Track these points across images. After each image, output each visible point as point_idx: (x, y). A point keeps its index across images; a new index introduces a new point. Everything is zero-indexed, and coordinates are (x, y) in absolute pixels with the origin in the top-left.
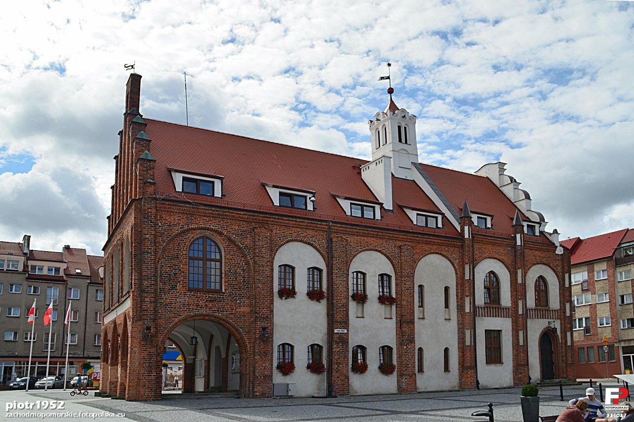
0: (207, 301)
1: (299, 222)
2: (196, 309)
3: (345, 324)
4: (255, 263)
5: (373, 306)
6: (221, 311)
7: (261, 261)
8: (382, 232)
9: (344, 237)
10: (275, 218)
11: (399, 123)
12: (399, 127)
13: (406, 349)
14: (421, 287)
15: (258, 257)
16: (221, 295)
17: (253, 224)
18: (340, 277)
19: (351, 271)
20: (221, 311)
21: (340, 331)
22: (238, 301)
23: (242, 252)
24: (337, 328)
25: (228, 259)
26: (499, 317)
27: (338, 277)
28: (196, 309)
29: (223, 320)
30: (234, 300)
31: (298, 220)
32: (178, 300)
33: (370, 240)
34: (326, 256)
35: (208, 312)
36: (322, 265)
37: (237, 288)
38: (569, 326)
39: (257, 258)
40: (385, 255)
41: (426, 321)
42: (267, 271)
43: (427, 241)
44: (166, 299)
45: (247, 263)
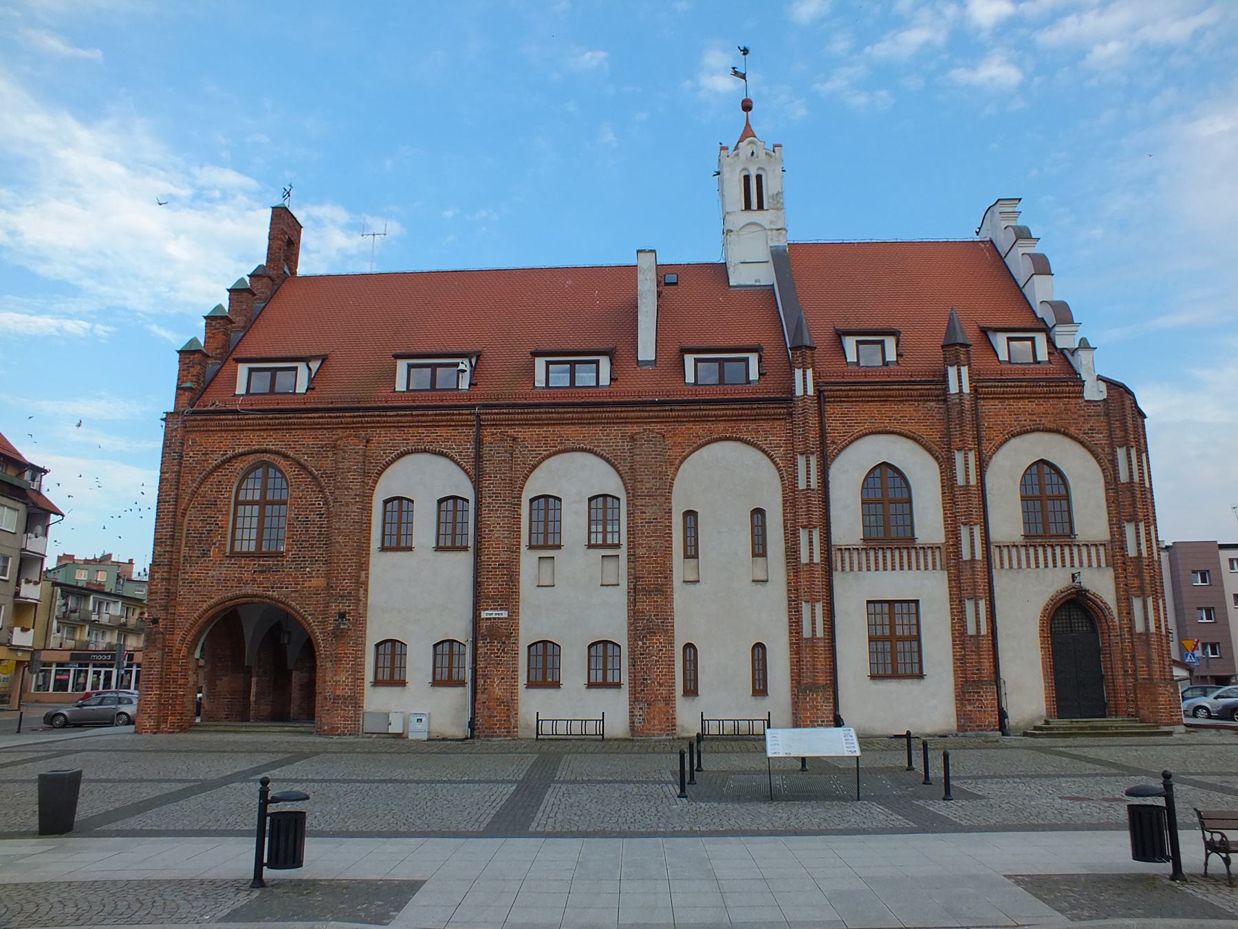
0: (255, 571)
1: (418, 415)
2: (236, 587)
3: (509, 597)
6: (277, 588)
7: (345, 495)
9: (510, 432)
10: (375, 416)
11: (744, 169)
12: (747, 178)
13: (643, 647)
14: (690, 515)
15: (339, 489)
16: (278, 561)
19: (527, 495)
20: (277, 588)
21: (494, 614)
22: (308, 569)
23: (319, 484)
24: (487, 609)
25: (295, 498)
26: (885, 569)
27: (493, 510)
28: (236, 587)
29: (281, 602)
31: (414, 413)
32: (210, 573)
33: (568, 430)
34: (472, 472)
35: (260, 591)
36: (465, 489)
37: (307, 547)
38: (1136, 582)
39: (337, 492)
40: (601, 456)
42: (355, 512)
43: (696, 417)
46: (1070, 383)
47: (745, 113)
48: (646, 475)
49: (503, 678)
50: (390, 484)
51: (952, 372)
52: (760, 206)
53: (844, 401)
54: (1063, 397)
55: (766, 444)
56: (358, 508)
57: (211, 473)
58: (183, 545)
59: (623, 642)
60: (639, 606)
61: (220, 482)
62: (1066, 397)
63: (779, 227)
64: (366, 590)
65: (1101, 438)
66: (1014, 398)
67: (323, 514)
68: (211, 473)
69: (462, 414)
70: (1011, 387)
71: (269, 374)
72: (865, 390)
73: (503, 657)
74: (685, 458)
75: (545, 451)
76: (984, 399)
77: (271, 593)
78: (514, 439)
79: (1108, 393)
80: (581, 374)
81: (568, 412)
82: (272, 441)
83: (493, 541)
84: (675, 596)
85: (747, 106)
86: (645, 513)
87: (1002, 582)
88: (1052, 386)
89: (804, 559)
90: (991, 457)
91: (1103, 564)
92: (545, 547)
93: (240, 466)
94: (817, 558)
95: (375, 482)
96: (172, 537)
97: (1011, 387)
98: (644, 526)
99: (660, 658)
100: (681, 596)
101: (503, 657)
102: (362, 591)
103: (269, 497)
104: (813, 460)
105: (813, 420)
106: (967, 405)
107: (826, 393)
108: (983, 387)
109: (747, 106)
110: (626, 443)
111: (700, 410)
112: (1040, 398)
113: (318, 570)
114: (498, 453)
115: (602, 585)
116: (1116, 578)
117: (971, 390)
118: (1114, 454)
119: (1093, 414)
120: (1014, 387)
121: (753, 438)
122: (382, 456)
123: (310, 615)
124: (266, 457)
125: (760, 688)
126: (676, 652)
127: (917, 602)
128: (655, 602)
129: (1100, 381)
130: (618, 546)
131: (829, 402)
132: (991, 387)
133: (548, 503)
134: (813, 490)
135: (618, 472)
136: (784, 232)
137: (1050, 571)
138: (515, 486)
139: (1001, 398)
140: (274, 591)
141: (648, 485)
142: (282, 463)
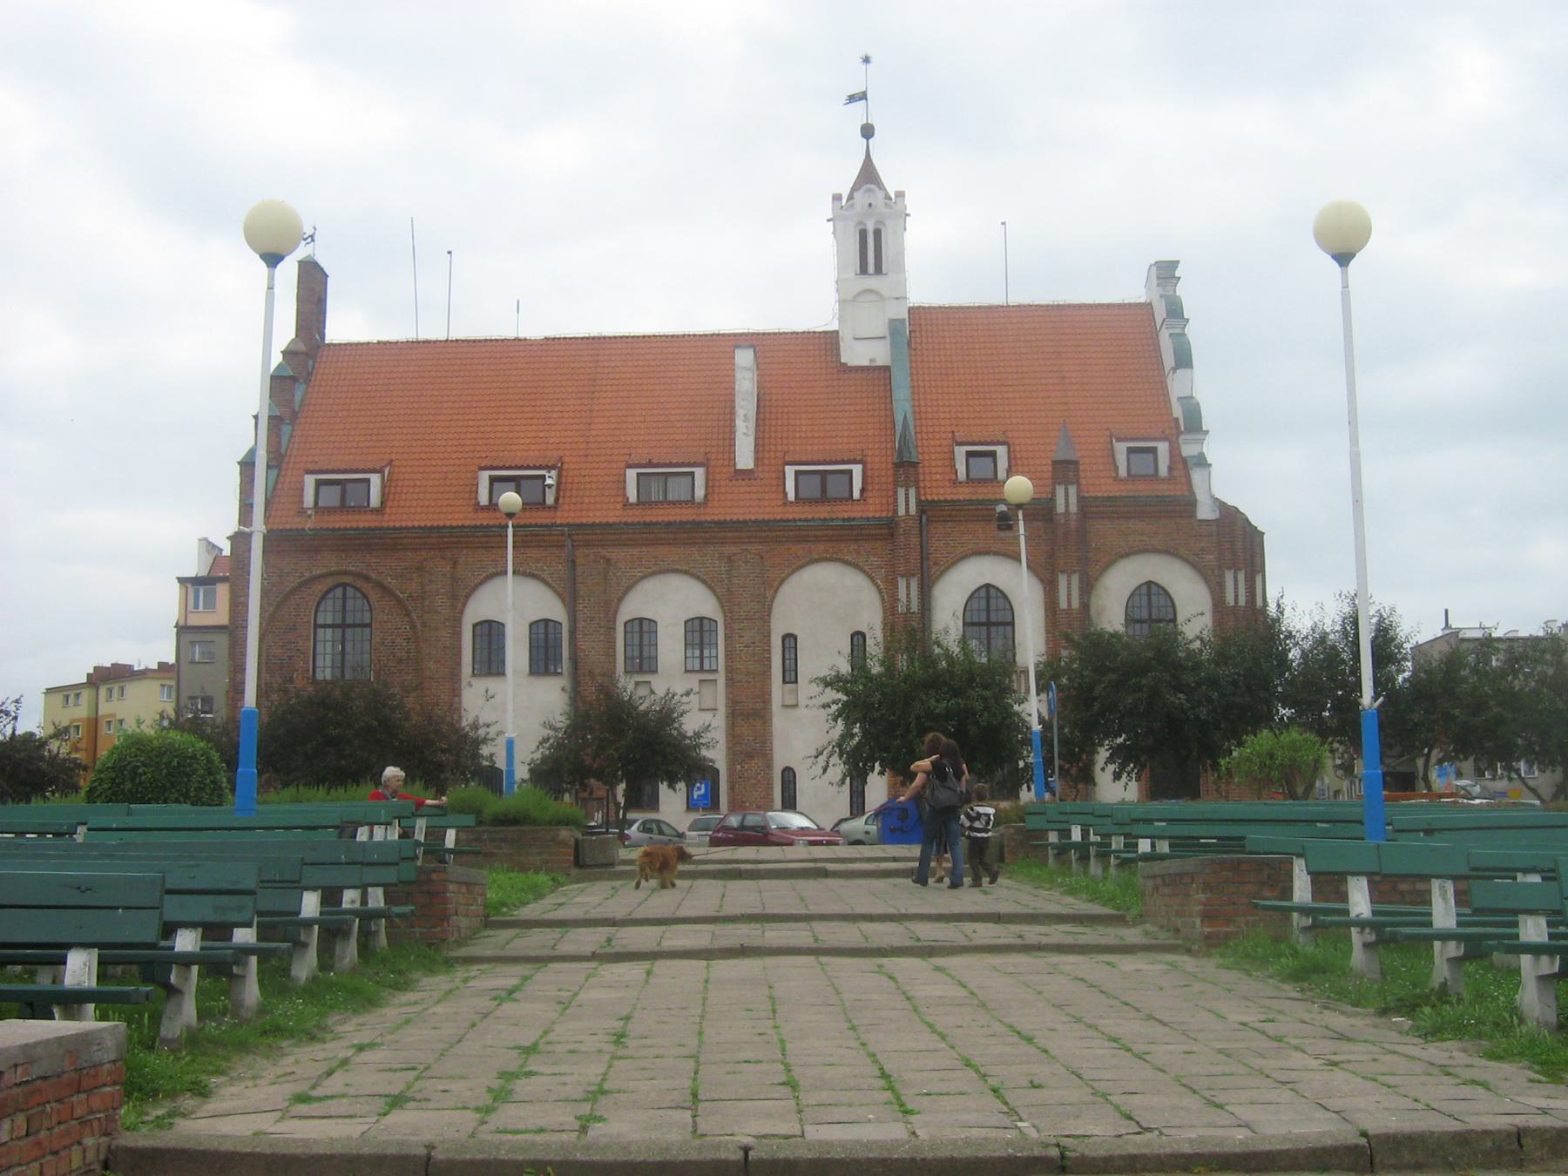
4: (424, 624)
9: (604, 553)
11: (860, 223)
12: (863, 234)
14: (790, 640)
17: (423, 552)
39: (426, 616)
40: (698, 578)
45: (413, 627)
47: (865, 140)
50: (483, 605)
51: (1060, 491)
52: (879, 270)
60: (737, 731)
65: (1210, 559)
71: (338, 489)
78: (608, 561)
84: (774, 720)
85: (867, 132)
90: (1096, 579)
92: (641, 671)
95: (464, 605)
103: (349, 620)
105: (915, 540)
109: (867, 132)
115: (700, 710)
118: (1222, 576)
124: (346, 579)
130: (716, 671)
133: (644, 629)
138: (610, 609)
142: (366, 587)
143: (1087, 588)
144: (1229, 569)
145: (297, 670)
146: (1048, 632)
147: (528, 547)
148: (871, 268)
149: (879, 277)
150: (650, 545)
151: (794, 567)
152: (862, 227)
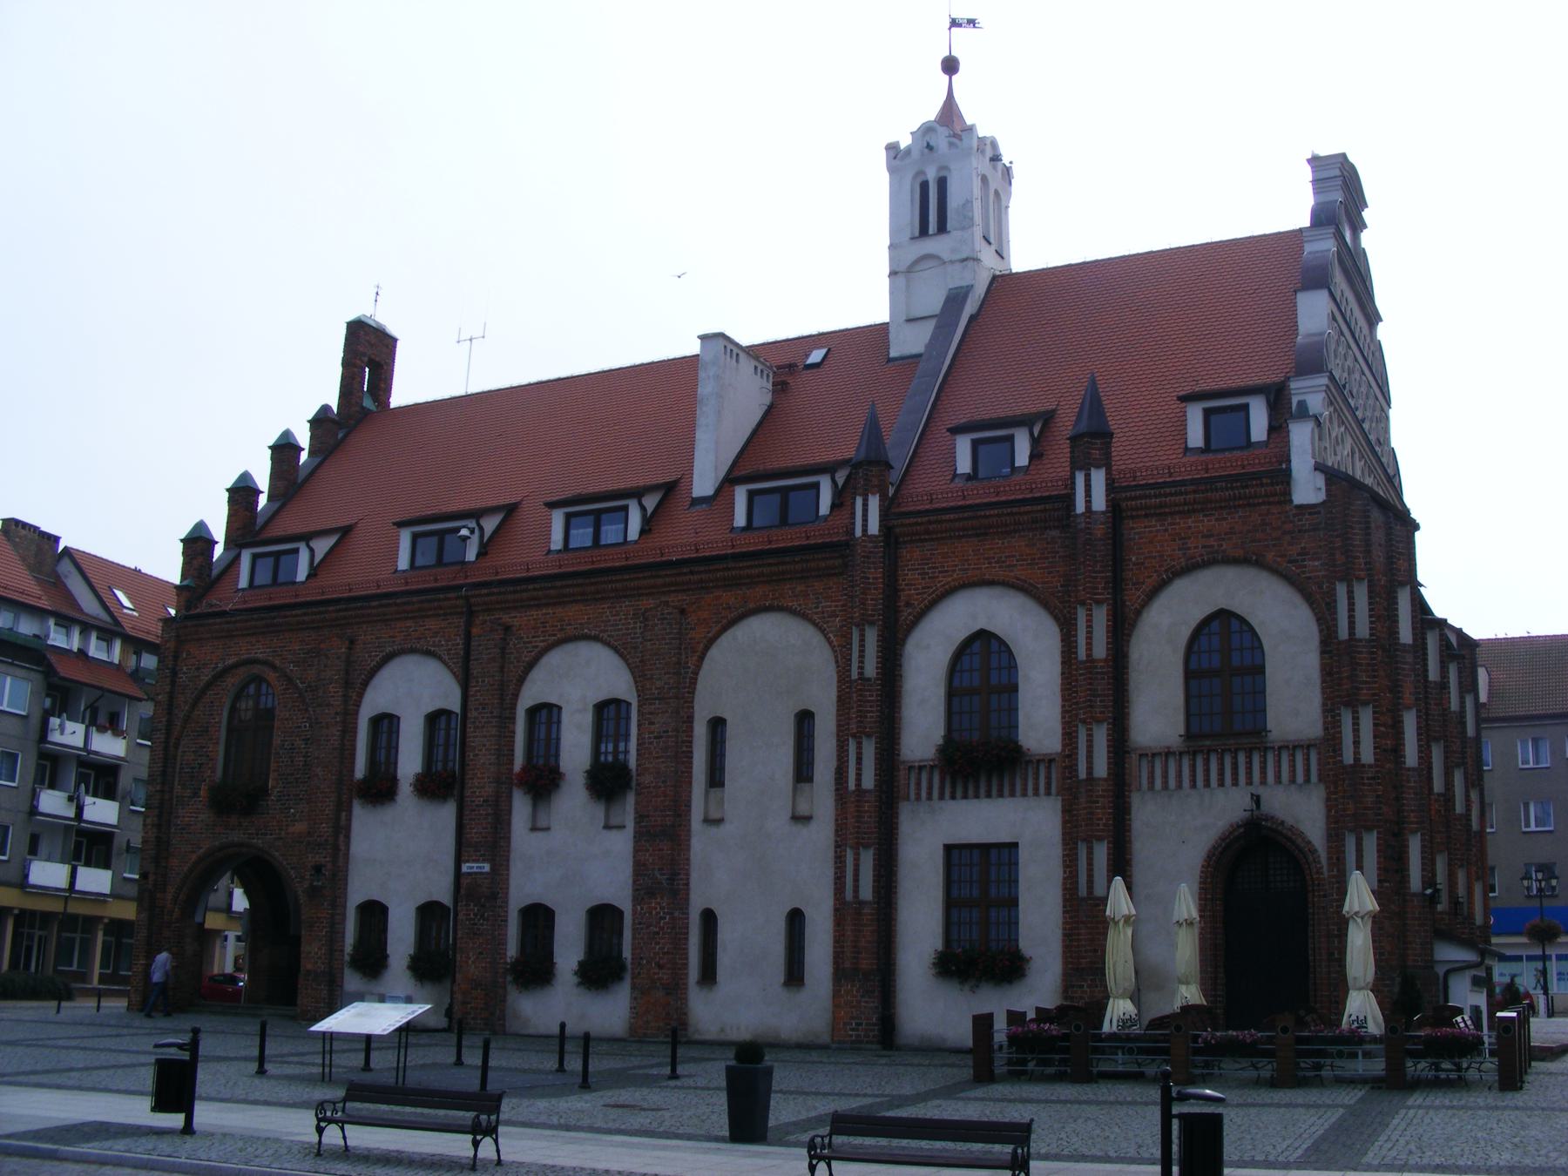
1: (404, 604)
5: (573, 800)
8: (592, 584)
9: (506, 618)
11: (921, 172)
12: (924, 186)
14: (717, 725)
18: (483, 727)
20: (262, 834)
22: (292, 811)
24: (468, 861)
27: (478, 727)
30: (286, 809)
40: (608, 644)
41: (726, 828)
44: (184, 817)
46: (1265, 481)
47: (947, 77)
48: (657, 669)
49: (481, 953)
50: (381, 696)
52: (942, 228)
53: (926, 540)
54: (1259, 504)
55: (816, 613)
56: (338, 731)
57: (203, 692)
58: (176, 783)
59: (626, 906)
61: (212, 702)
62: (1264, 503)
63: (964, 256)
64: (348, 837)
66: (1180, 512)
67: (308, 739)
68: (203, 692)
69: (449, 599)
70: (1171, 494)
72: (951, 521)
73: (482, 925)
74: (711, 641)
75: (543, 641)
76: (1132, 517)
77: (255, 841)
78: (507, 628)
79: (1327, 490)
80: (609, 527)
81: (568, 586)
82: (259, 649)
83: (478, 769)
85: (950, 66)
86: (653, 723)
87: (1146, 813)
88: (1237, 488)
89: (852, 785)
90: (1138, 613)
91: (1314, 778)
93: (232, 682)
94: (869, 782)
95: (361, 695)
96: (164, 773)
97: (1171, 494)
98: (651, 743)
99: (662, 928)
100: (701, 842)
101: (482, 925)
102: (342, 838)
104: (872, 636)
106: (1100, 530)
107: (897, 530)
108: (1127, 499)
109: (950, 66)
110: (638, 624)
111: (729, 569)
112: (1221, 508)
113: (302, 812)
114: (487, 649)
116: (1328, 799)
117: (1107, 506)
118: (1332, 594)
119: (1307, 527)
120: (1176, 494)
121: (800, 605)
122: (366, 661)
123: (292, 868)
124: (256, 669)
125: (794, 975)
126: (691, 921)
127: (1015, 845)
128: (660, 850)
129: (1317, 473)
131: (905, 542)
132: (1141, 497)
133: (546, 715)
134: (869, 679)
135: (628, 665)
136: (970, 263)
137: (1220, 795)
138: (507, 694)
139: (1160, 514)
140: (258, 839)
141: (659, 684)
143: (1122, 629)
144: (1341, 580)
145: (205, 781)
146: (1064, 699)
147: (428, 617)
148: (932, 227)
149: (944, 239)
150: (555, 604)
151: (725, 621)
152: (919, 180)
